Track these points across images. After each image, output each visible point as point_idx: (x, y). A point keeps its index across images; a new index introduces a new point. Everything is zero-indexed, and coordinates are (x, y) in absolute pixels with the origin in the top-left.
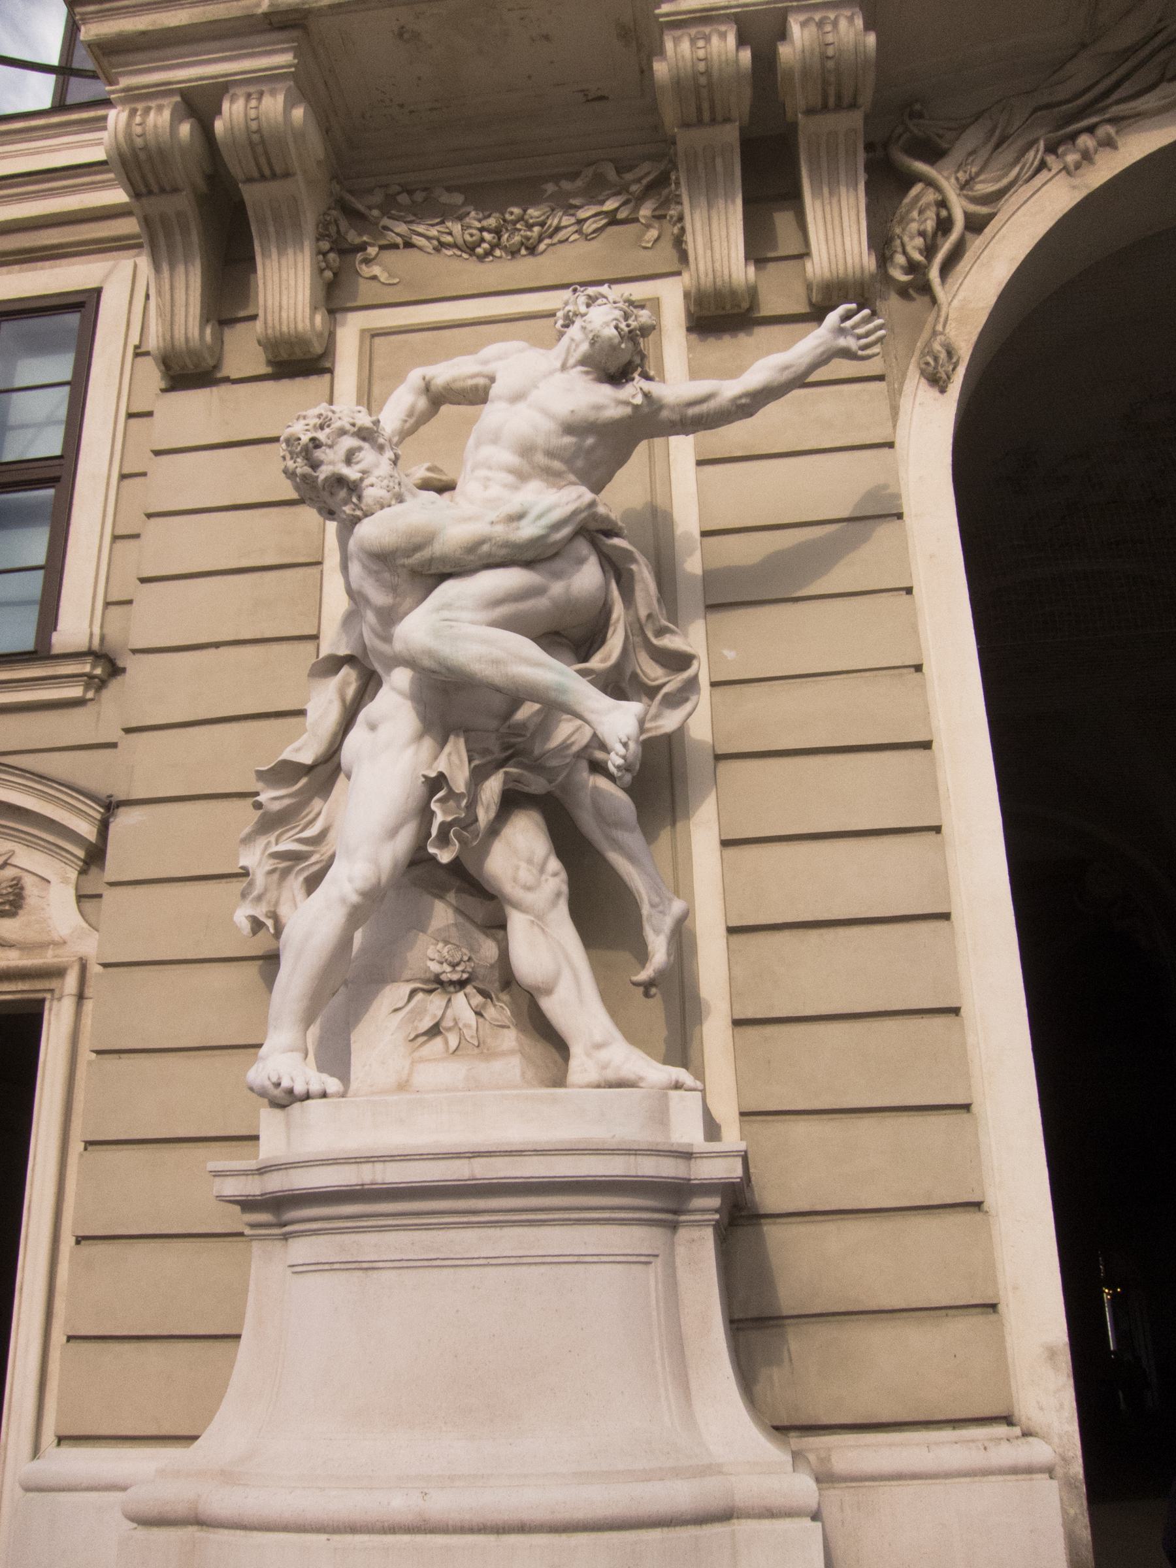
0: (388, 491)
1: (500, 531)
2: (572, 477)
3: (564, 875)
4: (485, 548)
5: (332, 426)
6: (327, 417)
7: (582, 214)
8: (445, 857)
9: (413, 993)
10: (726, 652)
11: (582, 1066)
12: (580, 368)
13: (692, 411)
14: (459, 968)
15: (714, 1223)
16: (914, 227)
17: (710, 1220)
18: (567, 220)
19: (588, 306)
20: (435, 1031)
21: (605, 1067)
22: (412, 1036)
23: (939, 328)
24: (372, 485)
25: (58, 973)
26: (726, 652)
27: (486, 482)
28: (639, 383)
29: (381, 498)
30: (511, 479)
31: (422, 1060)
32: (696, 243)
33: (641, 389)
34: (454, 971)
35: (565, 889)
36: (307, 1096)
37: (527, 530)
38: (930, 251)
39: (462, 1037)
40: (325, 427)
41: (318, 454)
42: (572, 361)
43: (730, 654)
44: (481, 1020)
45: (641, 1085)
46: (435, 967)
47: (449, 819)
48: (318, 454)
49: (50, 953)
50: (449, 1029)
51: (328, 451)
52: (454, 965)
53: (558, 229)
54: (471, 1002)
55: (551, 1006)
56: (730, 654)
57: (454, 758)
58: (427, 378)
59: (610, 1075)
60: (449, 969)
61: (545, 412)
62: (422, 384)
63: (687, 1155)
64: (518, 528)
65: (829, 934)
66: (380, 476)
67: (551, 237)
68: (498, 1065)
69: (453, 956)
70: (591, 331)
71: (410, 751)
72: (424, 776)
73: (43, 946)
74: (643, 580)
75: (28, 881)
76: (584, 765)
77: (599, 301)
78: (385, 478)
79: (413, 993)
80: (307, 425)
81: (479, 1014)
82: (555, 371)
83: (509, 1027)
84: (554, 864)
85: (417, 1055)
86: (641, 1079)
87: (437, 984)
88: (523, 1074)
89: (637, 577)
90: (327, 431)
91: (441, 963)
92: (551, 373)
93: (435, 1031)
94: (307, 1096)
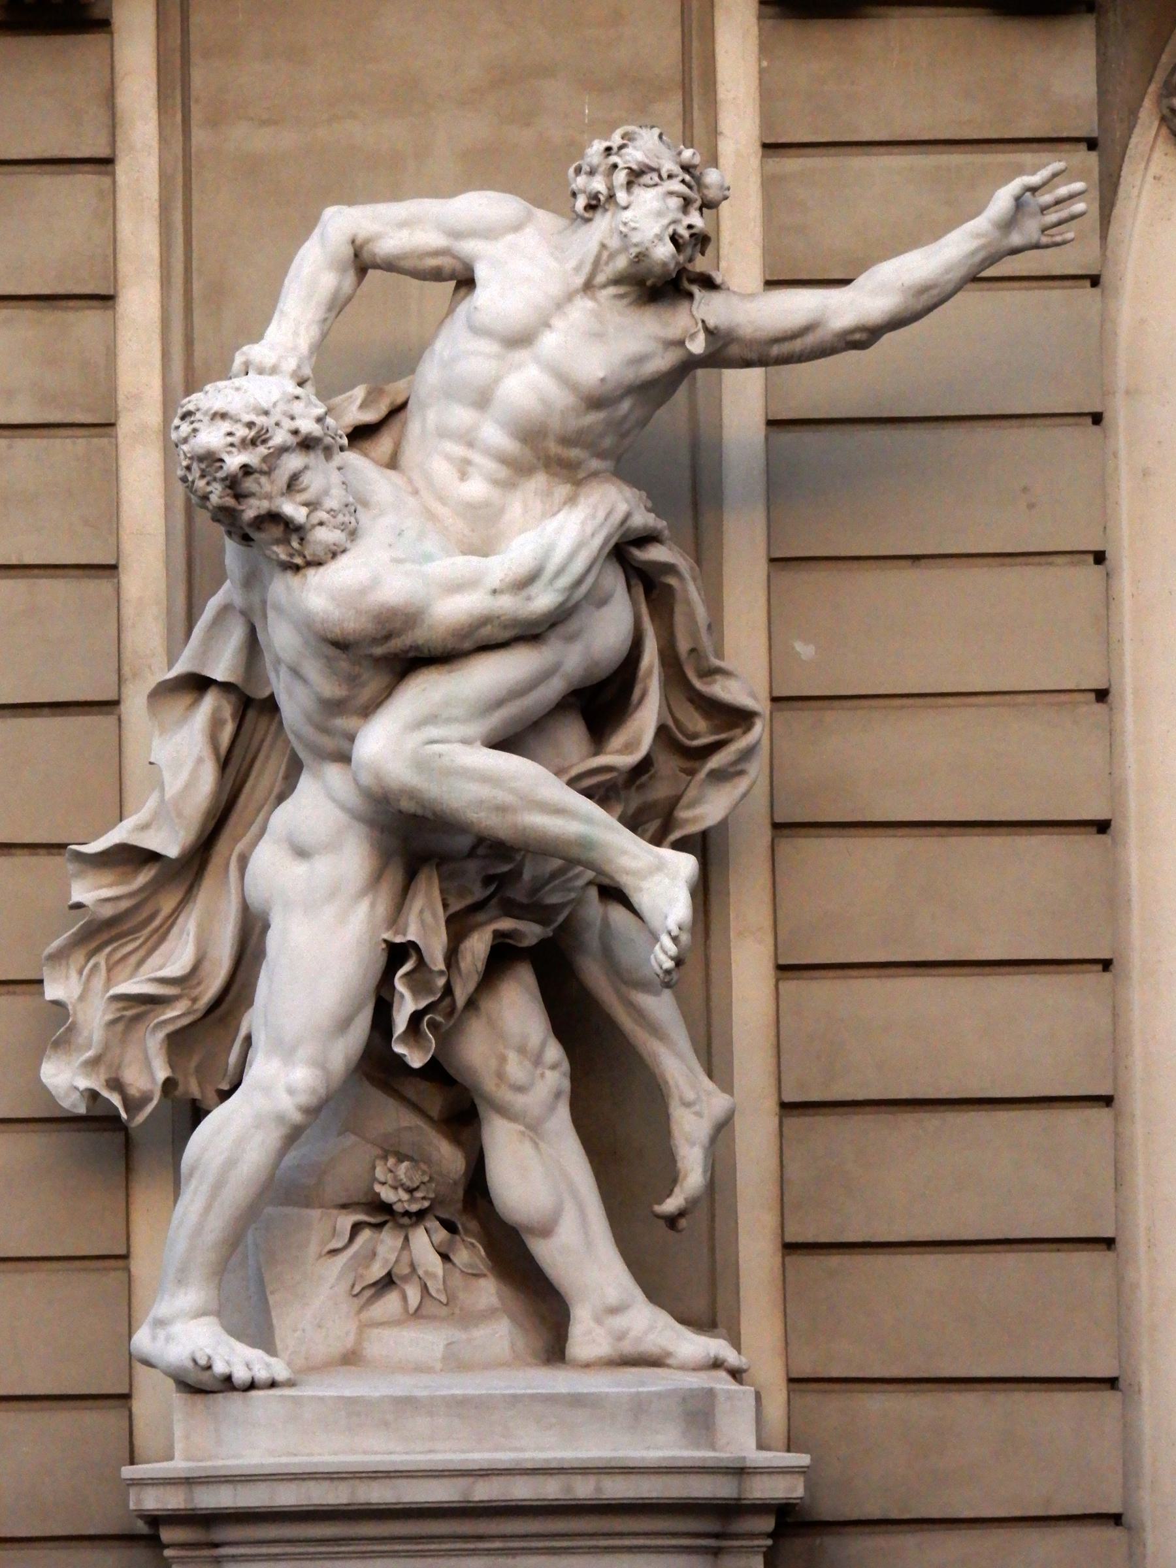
0: (342, 530)
1: (507, 604)
2: (595, 464)
3: (566, 1066)
5: (271, 443)
6: (262, 429)
8: (416, 1060)
9: (356, 1228)
10: (799, 646)
12: (612, 290)
13: (775, 350)
14: (419, 1194)
15: (765, 1549)
17: (759, 1546)
19: (629, 185)
20: (388, 1282)
21: (621, 1337)
22: (357, 1289)
24: (321, 524)
26: (799, 646)
27: (463, 469)
29: (335, 545)
30: (503, 472)
33: (703, 321)
34: (412, 1199)
35: (566, 1084)
36: (252, 1386)
39: (425, 1289)
40: (258, 443)
41: (249, 484)
42: (601, 278)
43: (805, 650)
44: (449, 1266)
45: (669, 1361)
46: (387, 1195)
47: (422, 1004)
48: (249, 484)
50: (406, 1279)
51: (263, 480)
52: (411, 1191)
54: (434, 1239)
55: (545, 1252)
56: (805, 650)
57: (428, 916)
58: (358, 242)
59: (627, 1347)
60: (405, 1196)
61: (563, 378)
62: (348, 251)
63: (740, 1471)
64: (529, 598)
65: (932, 1120)
66: (332, 510)
68: (481, 1333)
69: (411, 1179)
70: (636, 245)
71: (363, 907)
72: (385, 941)
74: (688, 602)
76: (593, 893)
77: (646, 179)
78: (340, 511)
79: (356, 1228)
80: (230, 434)
81: (445, 1257)
82: (576, 292)
83: (485, 1276)
84: (554, 1052)
85: (365, 1315)
86: (669, 1354)
88: (513, 1345)
89: (679, 595)
90: (262, 450)
91: (395, 1188)
92: (570, 297)
93: (388, 1282)
94: (252, 1386)
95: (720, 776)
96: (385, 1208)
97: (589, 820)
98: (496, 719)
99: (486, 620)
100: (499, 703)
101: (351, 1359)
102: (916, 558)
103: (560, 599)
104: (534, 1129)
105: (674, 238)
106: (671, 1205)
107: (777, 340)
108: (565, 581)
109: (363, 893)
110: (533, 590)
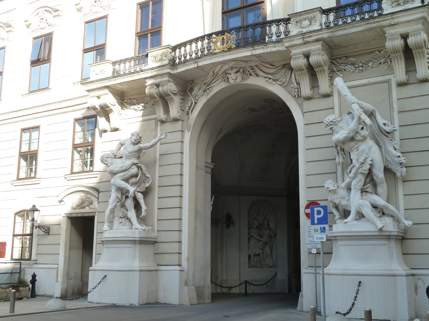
4: (119, 171)
7: (149, 104)
9: (119, 218)
11: (133, 228)
13: (145, 148)
16: (187, 105)
18: (147, 105)
23: (189, 122)
25: (95, 212)
28: (140, 145)
31: (119, 226)
32: (157, 112)
37: (124, 168)
38: (189, 110)
43: (161, 172)
46: (121, 216)
49: (95, 210)
53: (146, 106)
56: (161, 172)
59: (136, 228)
62: (120, 143)
67: (146, 107)
71: (115, 193)
73: (94, 209)
75: (93, 200)
81: (125, 221)
87: (121, 218)
93: (121, 222)
95: (148, 182)
96: (121, 217)
97: (126, 185)
98: (121, 178)
99: (119, 170)
100: (121, 177)
101: (117, 229)
102: (168, 165)
103: (125, 168)
104: (130, 211)
105: (135, 140)
106: (141, 216)
107: (145, 147)
108: (126, 167)
109: (115, 192)
110: (123, 168)
